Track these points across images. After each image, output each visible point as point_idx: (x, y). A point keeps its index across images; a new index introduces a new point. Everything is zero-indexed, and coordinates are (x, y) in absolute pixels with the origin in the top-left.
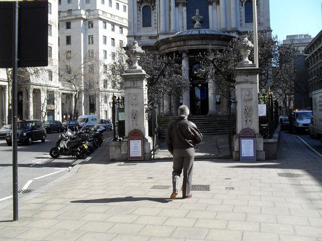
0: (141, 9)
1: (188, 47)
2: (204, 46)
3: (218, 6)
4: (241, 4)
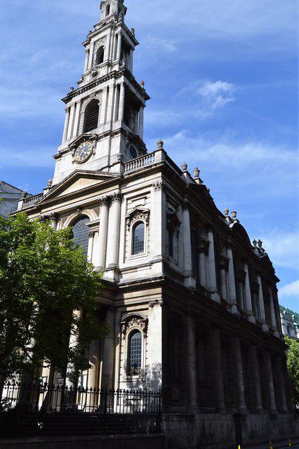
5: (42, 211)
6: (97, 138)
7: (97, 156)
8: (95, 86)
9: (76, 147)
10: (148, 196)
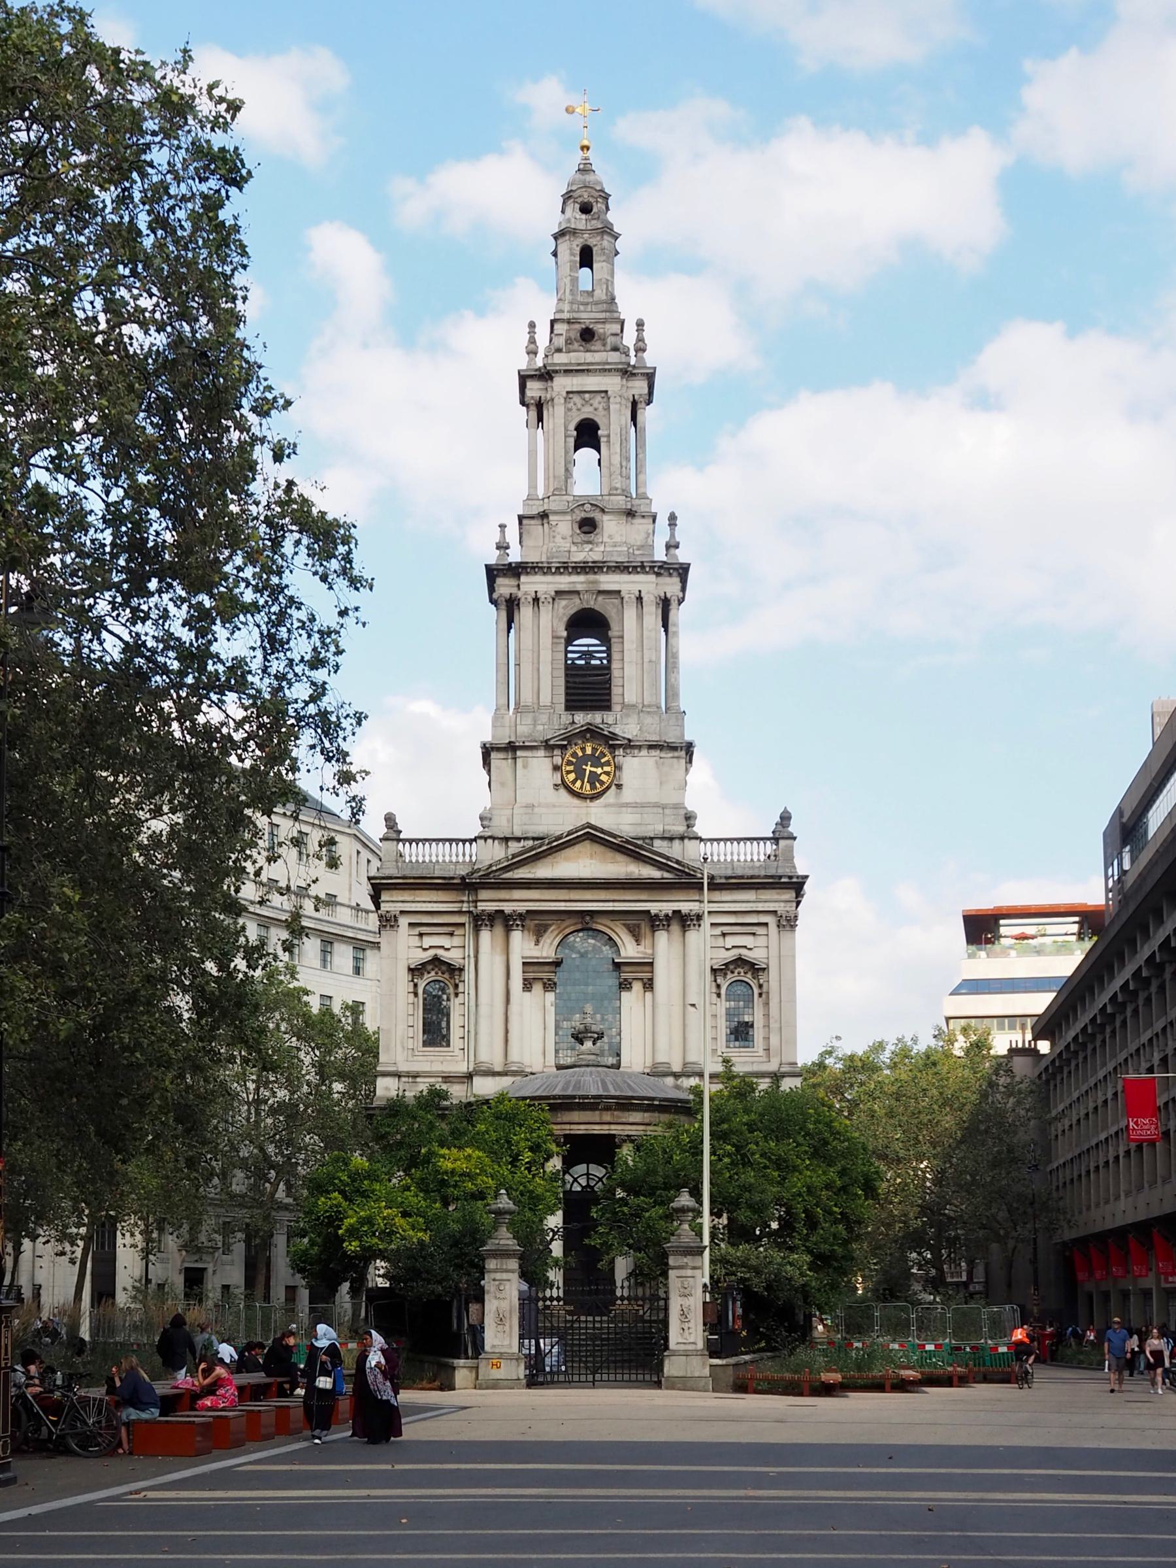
0: (420, 991)
1: (564, 1127)
2: (606, 1127)
3: (648, 994)
4: (714, 990)
5: (484, 894)
6: (630, 746)
7: (628, 795)
8: (595, 573)
9: (563, 748)
10: (760, 930)
